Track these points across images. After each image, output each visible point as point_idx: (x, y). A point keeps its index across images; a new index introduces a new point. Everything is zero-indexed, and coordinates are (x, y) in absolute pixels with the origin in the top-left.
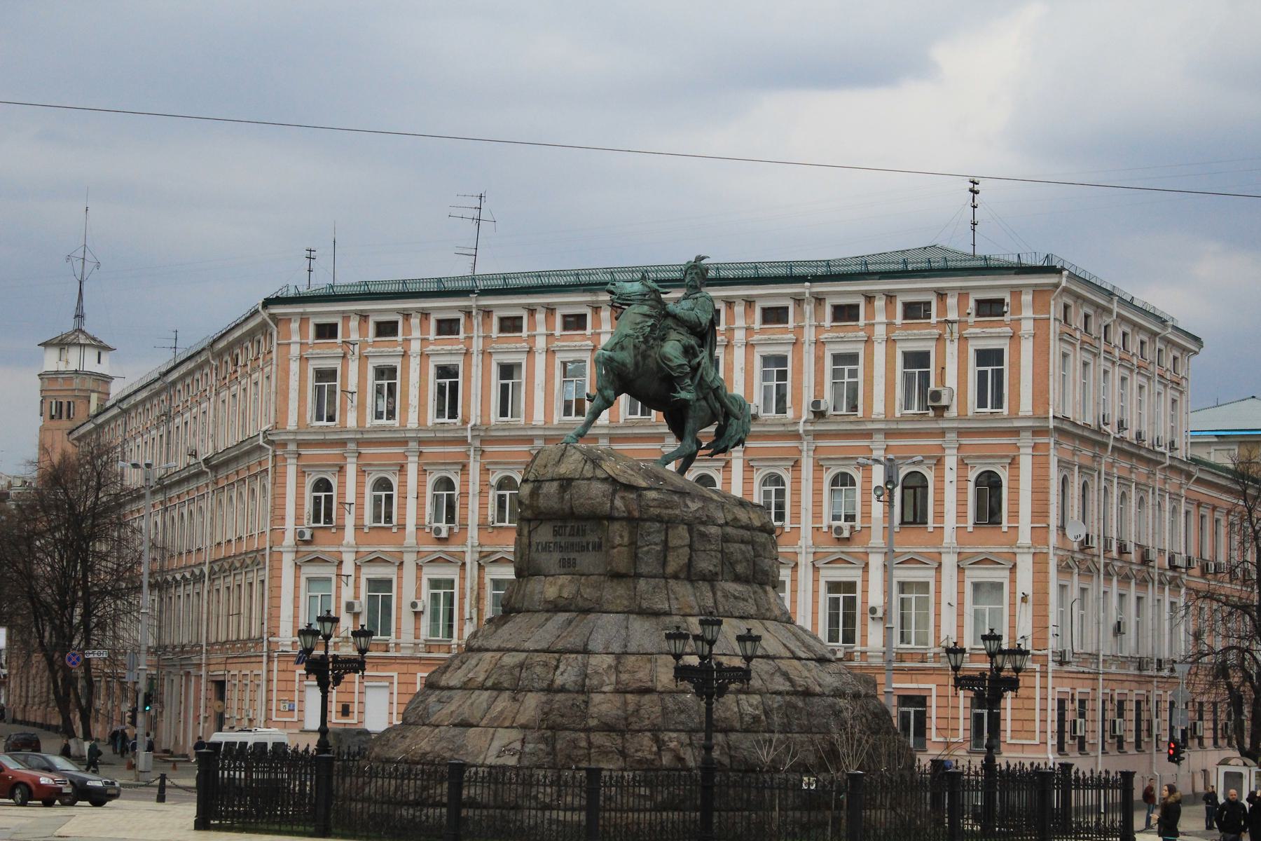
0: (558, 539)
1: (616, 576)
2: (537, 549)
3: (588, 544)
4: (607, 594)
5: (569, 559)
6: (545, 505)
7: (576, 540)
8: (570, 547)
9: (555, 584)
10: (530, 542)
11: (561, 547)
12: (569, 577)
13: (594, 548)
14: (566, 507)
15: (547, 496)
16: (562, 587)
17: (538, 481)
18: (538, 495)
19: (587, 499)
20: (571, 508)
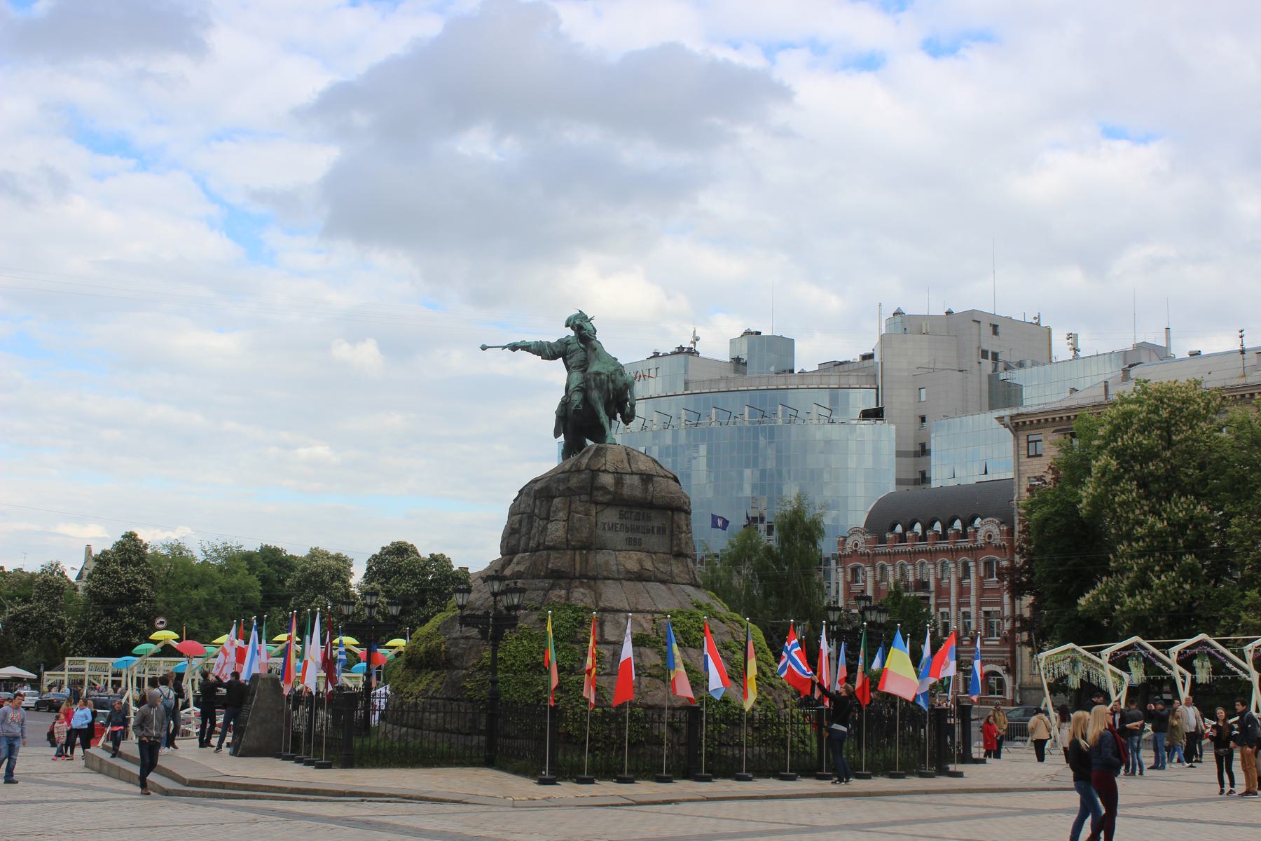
0: (624, 521)
1: (680, 555)
2: (604, 528)
3: (653, 528)
4: (676, 571)
5: (635, 538)
6: (629, 493)
7: (640, 523)
8: (637, 530)
9: (630, 558)
10: (596, 522)
11: (627, 528)
12: (644, 554)
13: (658, 531)
14: (649, 498)
15: (631, 486)
16: (640, 561)
17: (617, 473)
18: (623, 485)
19: (668, 493)
20: (652, 500)
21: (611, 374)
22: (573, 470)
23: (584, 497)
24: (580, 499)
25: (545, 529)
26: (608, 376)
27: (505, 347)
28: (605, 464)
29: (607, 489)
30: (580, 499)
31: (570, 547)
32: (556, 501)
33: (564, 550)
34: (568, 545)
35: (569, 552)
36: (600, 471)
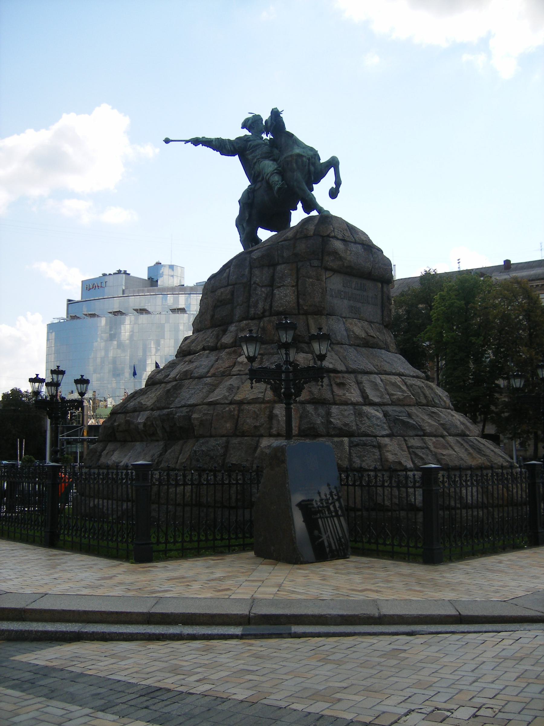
21: (312, 158)
22: (298, 237)
23: (316, 263)
24: (310, 264)
25: (271, 295)
26: (309, 159)
27: (187, 142)
28: (334, 231)
29: (339, 254)
30: (310, 264)
31: (301, 312)
32: (279, 268)
33: (295, 315)
34: (299, 309)
35: (301, 317)
36: (330, 237)
